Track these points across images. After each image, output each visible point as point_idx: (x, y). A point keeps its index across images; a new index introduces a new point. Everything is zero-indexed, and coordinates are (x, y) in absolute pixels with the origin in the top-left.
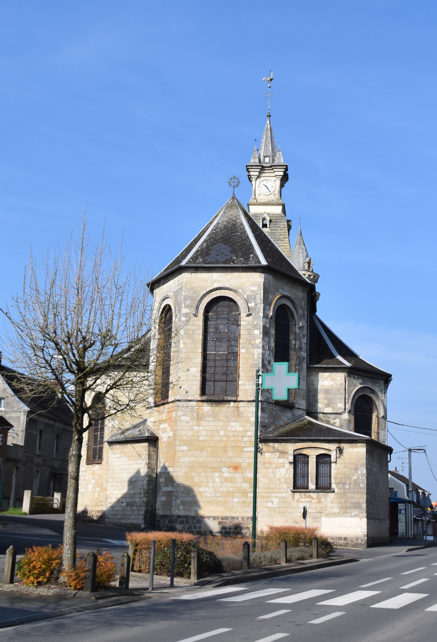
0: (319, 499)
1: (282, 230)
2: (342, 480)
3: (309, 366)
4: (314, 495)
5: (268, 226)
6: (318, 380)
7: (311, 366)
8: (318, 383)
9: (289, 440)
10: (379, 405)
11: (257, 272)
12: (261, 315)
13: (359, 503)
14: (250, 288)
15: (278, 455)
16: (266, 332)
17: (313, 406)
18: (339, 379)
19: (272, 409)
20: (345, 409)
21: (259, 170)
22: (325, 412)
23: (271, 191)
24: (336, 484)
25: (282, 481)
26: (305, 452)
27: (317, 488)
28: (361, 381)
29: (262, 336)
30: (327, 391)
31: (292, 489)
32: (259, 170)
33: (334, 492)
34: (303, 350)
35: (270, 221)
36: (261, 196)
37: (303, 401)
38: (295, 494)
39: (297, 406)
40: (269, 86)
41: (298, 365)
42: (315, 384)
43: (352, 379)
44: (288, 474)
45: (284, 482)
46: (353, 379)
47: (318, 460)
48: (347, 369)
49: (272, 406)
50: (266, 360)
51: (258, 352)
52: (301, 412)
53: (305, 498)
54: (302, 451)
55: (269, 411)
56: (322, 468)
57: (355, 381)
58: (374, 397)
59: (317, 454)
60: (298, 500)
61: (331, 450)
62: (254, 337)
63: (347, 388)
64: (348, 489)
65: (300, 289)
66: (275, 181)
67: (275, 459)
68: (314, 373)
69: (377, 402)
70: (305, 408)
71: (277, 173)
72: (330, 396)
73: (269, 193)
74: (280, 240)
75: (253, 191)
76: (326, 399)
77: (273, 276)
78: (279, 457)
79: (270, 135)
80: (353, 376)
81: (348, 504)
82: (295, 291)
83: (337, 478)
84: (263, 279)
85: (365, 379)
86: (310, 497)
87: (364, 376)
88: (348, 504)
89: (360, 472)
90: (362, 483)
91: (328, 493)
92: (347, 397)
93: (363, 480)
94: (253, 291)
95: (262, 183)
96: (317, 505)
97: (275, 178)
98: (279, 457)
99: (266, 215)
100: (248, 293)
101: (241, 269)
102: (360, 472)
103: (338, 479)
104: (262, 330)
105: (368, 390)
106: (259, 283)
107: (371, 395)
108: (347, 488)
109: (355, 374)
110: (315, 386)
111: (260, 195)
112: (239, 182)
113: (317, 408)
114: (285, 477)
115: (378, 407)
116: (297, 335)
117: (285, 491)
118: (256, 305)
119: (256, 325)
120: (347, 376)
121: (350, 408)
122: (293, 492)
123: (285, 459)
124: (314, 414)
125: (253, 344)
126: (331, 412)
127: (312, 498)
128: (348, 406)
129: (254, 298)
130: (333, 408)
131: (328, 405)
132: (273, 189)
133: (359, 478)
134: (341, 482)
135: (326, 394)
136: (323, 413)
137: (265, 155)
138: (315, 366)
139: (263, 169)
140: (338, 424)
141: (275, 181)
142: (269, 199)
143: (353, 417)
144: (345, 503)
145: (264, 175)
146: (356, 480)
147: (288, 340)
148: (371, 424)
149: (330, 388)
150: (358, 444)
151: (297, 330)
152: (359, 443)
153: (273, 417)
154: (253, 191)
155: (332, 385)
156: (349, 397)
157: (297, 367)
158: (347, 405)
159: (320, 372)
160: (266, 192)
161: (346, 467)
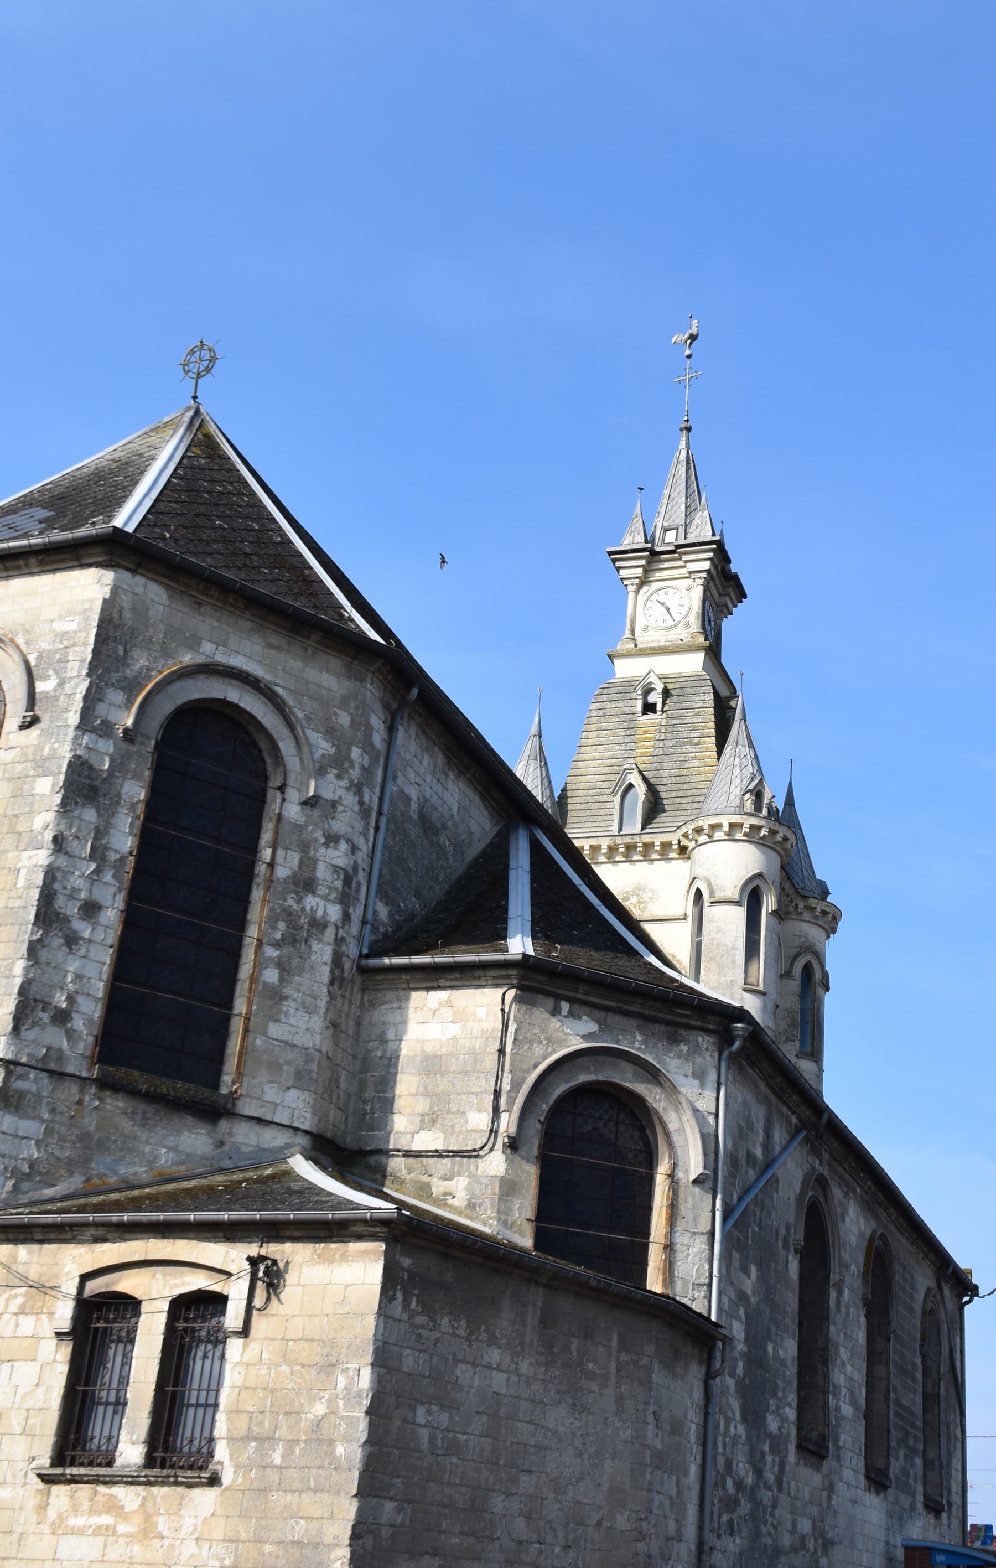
0: (148, 1517)
1: (697, 715)
2: (261, 1424)
3: (364, 962)
4: (128, 1496)
5: (659, 707)
6: (404, 1022)
7: (373, 962)
8: (405, 1032)
9: (73, 1226)
10: (682, 1130)
11: (90, 565)
12: (74, 718)
13: (317, 1545)
14: (55, 625)
15: (20, 1300)
16: (82, 786)
17: (372, 1128)
18: (481, 1013)
19: (80, 1102)
20: (493, 1132)
21: (643, 562)
22: (417, 1146)
23: (678, 617)
24: (230, 1439)
25: (14, 1423)
26: (126, 1284)
27: (150, 1461)
28: (593, 1027)
29: (58, 799)
30: (432, 1065)
31: (46, 1461)
32: (643, 562)
33: (214, 1481)
34: (322, 890)
35: (666, 693)
36: (650, 633)
37: (293, 1093)
38: (55, 1488)
39: (248, 1107)
40: (688, 352)
41: (277, 944)
42: (390, 1035)
43: (540, 1014)
44: (41, 1390)
45: (18, 1430)
46: (546, 1015)
47: (181, 1325)
48: (514, 972)
49: (82, 1091)
50: (71, 897)
51: (34, 862)
52: (273, 1139)
53: (92, 1512)
54: (115, 1283)
55: (53, 1111)
56: (199, 1363)
57: (555, 1023)
58: (654, 1097)
59: (177, 1292)
60: (61, 1518)
61: (229, 1274)
62: (32, 804)
63: (508, 1048)
64: (280, 1468)
65: (336, 663)
66: (689, 589)
67: (6, 1317)
68: (390, 995)
69: (672, 1121)
70: (306, 1126)
71: (692, 566)
72: (443, 1084)
73: (670, 622)
74: (691, 744)
75: (628, 620)
76: (426, 1094)
77: (167, 587)
78: (22, 1311)
79: (684, 475)
80: (550, 1002)
81: (268, 1548)
82: (299, 664)
83: (238, 1412)
84: (108, 589)
85: (614, 1019)
86: (114, 1507)
87: (607, 1009)
88: (268, 1548)
89: (342, 1382)
90: (347, 1439)
91: (190, 1486)
92: (506, 1086)
93: (350, 1421)
94: (63, 635)
95: (655, 597)
96: (136, 1548)
97: (690, 581)
98: (22, 1311)
99: (653, 678)
100: (44, 645)
101: (33, 561)
102: (342, 1382)
103: (245, 1417)
104: (62, 777)
105: (624, 1064)
106: (87, 606)
107: (640, 1088)
108: (278, 1461)
109: (558, 997)
110: (392, 1046)
111: (646, 629)
112: (213, 360)
113: (389, 1134)
114: (30, 1404)
115: (676, 1139)
116: (285, 827)
117: (14, 1476)
118: (61, 684)
119: (45, 760)
120: (516, 999)
121: (513, 1130)
122: (47, 1479)
123: (44, 1317)
124: (372, 1160)
125: (20, 833)
126: (440, 1147)
127: (114, 1507)
128: (508, 1123)
129: (60, 661)
130: (449, 1131)
131: (429, 1121)
132: (684, 610)
133: (333, 1412)
134: (256, 1430)
135: (428, 1075)
136: (408, 1154)
137: (666, 524)
138: (387, 961)
139: (656, 558)
140: (460, 1201)
141: (689, 589)
142: (670, 638)
143: (530, 1174)
144: (258, 1541)
145: (658, 575)
146: (318, 1422)
147: (253, 850)
148: (650, 1209)
149: (444, 1051)
150: (354, 1246)
151: (293, 811)
152: (359, 1237)
153: (85, 1137)
154: (628, 620)
155: (453, 1038)
156: (516, 1086)
157: (271, 952)
158: (504, 1117)
159: (416, 989)
160: (665, 621)
161: (285, 1357)
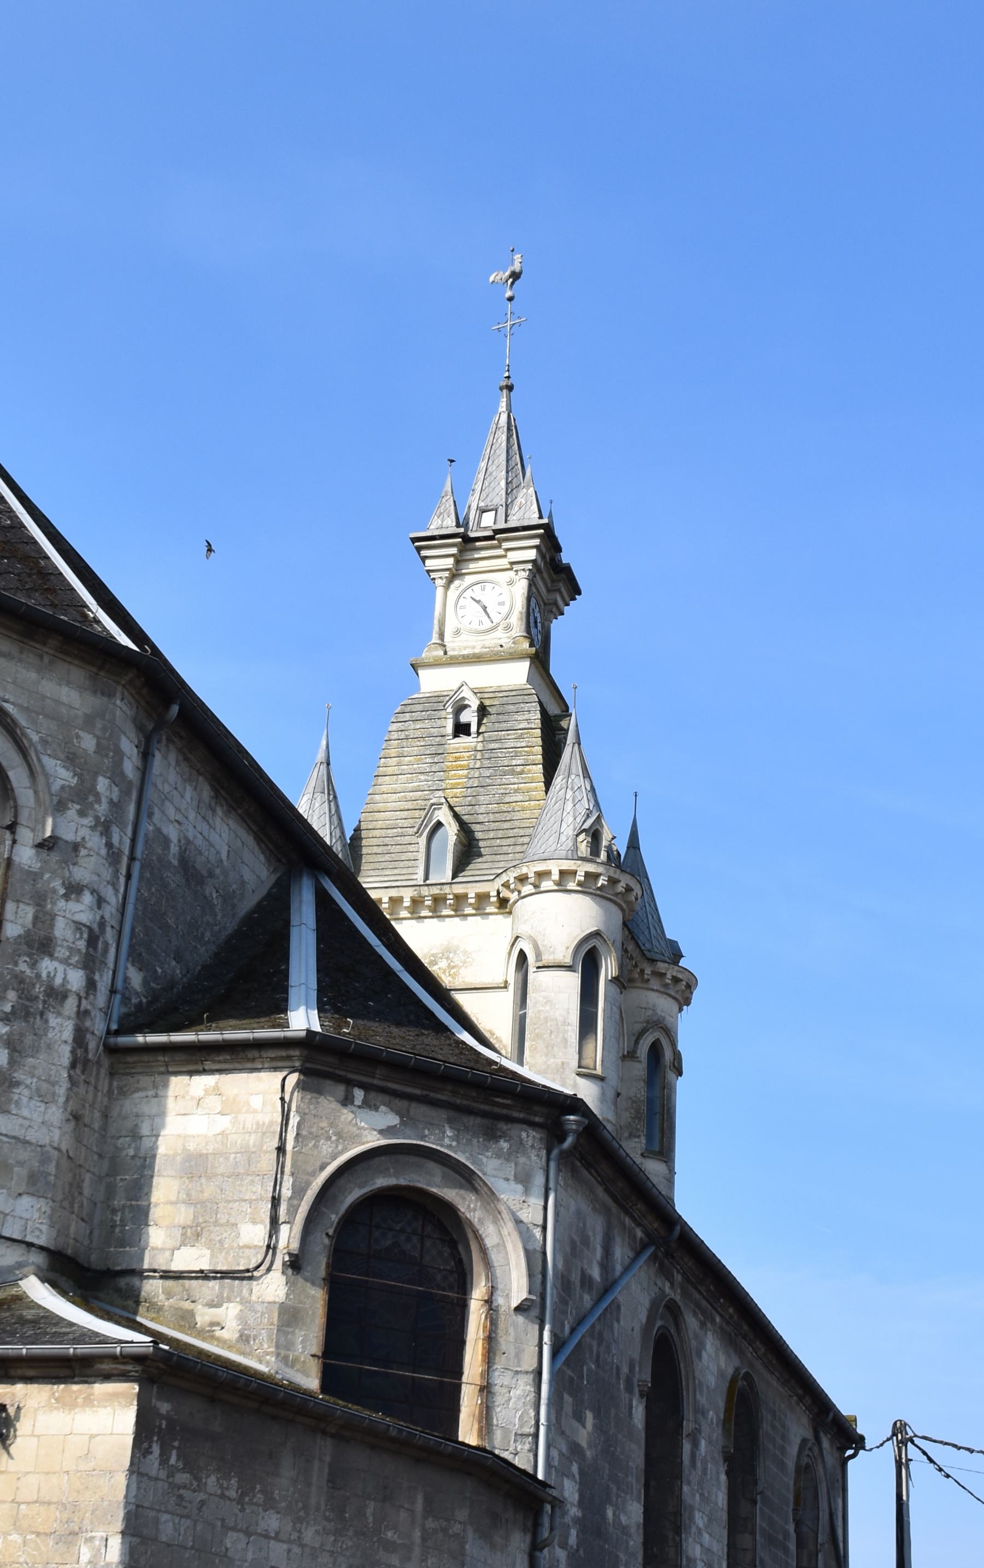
1: (520, 737)
3: (112, 1040)
5: (474, 728)
6: (162, 1114)
7: (124, 1040)
8: (163, 1126)
10: (501, 1245)
17: (122, 1243)
18: (256, 1102)
20: (271, 1248)
21: (454, 551)
22: (176, 1266)
23: (496, 618)
30: (196, 1166)
32: (454, 551)
34: (61, 952)
35: (483, 711)
36: (464, 637)
37: (26, 1201)
40: (509, 294)
42: (145, 1130)
43: (328, 1104)
46: (335, 1105)
48: (296, 1052)
57: (346, 1115)
58: (467, 1205)
63: (289, 1146)
65: (78, 674)
66: (511, 583)
68: (145, 1080)
70: (42, 1241)
71: (514, 556)
72: (209, 1190)
73: (488, 625)
74: (513, 773)
75: (436, 622)
76: (189, 1201)
79: (504, 444)
80: (341, 1089)
82: (33, 675)
85: (419, 1110)
89: (86, 1554)
92: (286, 1192)
95: (469, 593)
97: (512, 573)
99: (466, 693)
105: (431, 1165)
107: (450, 1194)
109: (350, 1084)
110: (146, 1143)
111: (457, 632)
113: (143, 1250)
115: (495, 1257)
116: (16, 876)
120: (299, 1085)
121: (295, 1246)
124: (123, 1282)
126: (205, 1267)
128: (289, 1237)
130: (217, 1247)
131: (192, 1234)
132: (504, 610)
135: (191, 1178)
136: (167, 1275)
137: (482, 504)
138: (140, 1039)
139: (470, 545)
140: (230, 1332)
141: (511, 583)
142: (487, 643)
143: (315, 1299)
145: (473, 566)
148: (463, 1343)
149: (210, 1149)
151: (26, 855)
152: (107, 1377)
154: (436, 622)
155: (222, 1133)
156: (299, 1192)
158: (284, 1230)
159: (176, 1073)
160: (481, 623)
161: (16, 1524)
